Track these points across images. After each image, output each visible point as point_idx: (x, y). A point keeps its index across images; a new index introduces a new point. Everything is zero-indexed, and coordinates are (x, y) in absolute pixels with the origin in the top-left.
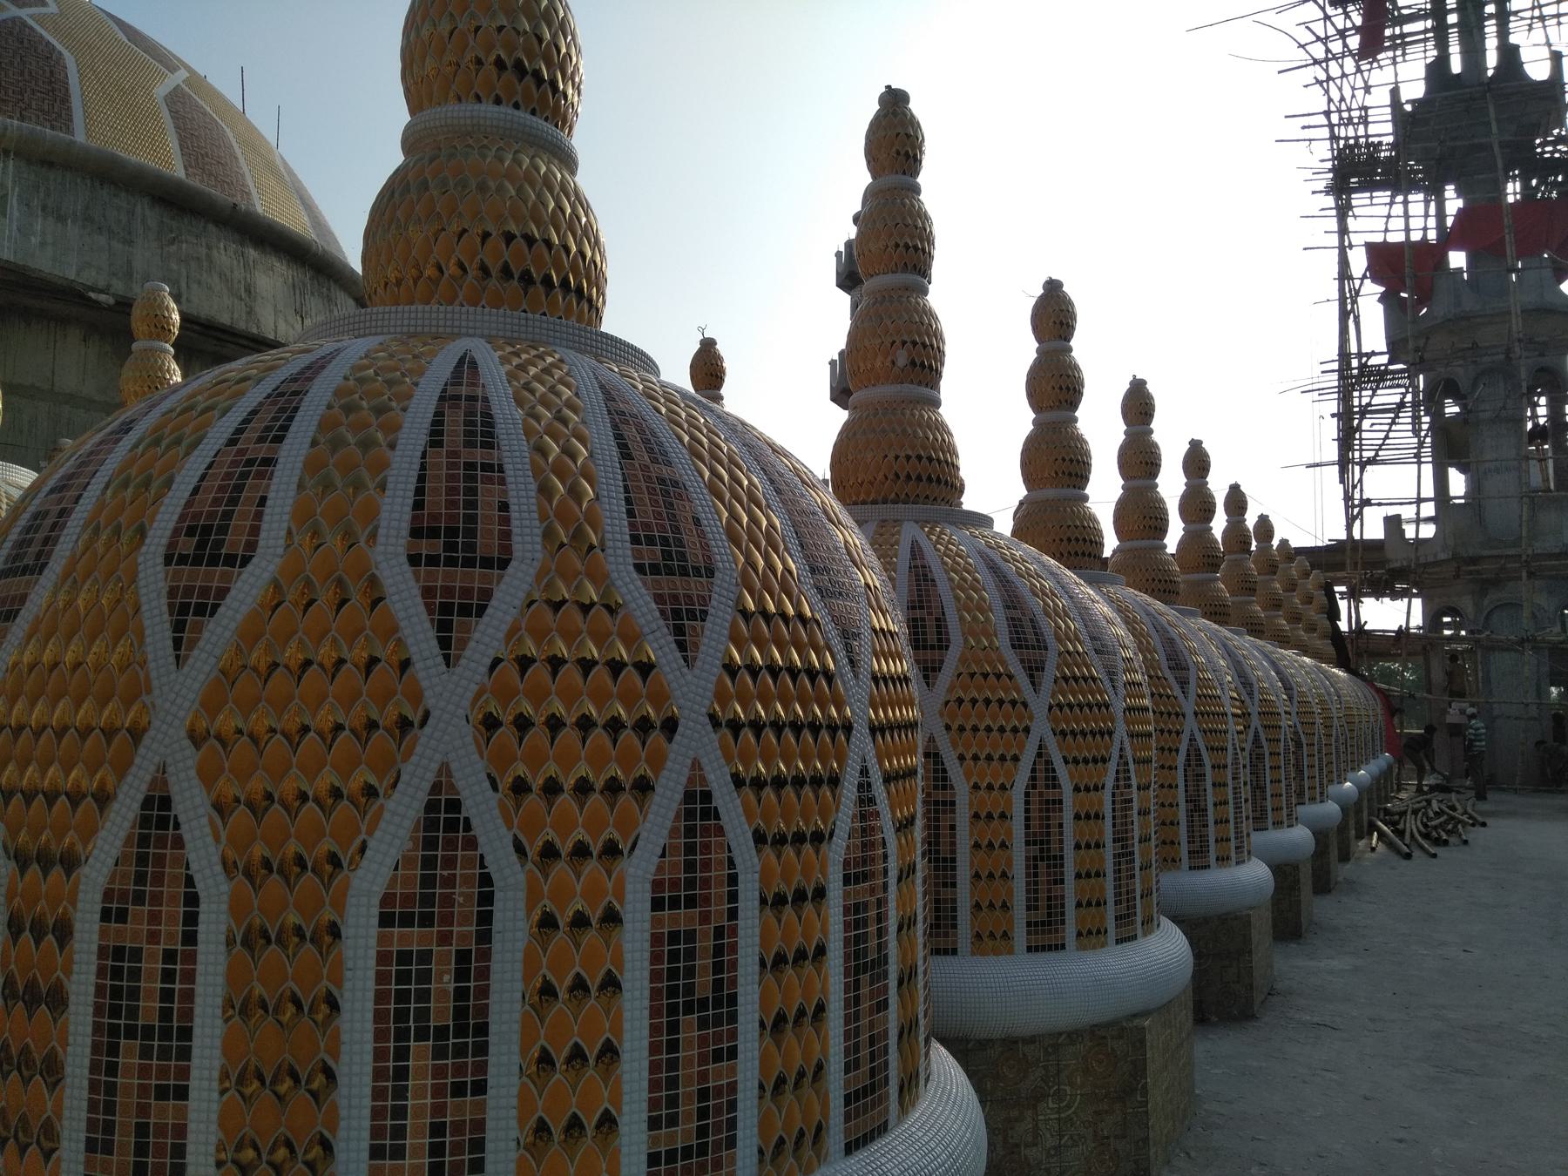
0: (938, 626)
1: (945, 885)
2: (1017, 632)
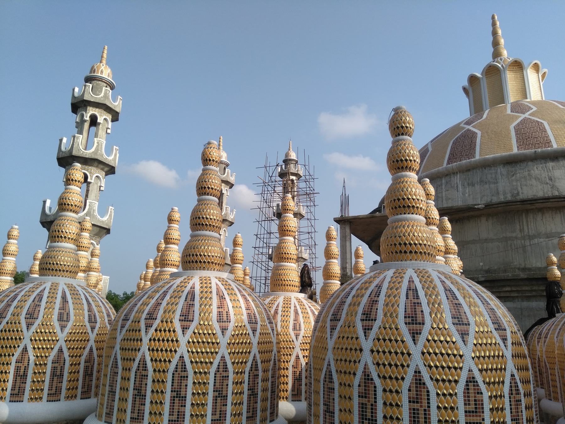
1: (224, 405)
2: (250, 318)
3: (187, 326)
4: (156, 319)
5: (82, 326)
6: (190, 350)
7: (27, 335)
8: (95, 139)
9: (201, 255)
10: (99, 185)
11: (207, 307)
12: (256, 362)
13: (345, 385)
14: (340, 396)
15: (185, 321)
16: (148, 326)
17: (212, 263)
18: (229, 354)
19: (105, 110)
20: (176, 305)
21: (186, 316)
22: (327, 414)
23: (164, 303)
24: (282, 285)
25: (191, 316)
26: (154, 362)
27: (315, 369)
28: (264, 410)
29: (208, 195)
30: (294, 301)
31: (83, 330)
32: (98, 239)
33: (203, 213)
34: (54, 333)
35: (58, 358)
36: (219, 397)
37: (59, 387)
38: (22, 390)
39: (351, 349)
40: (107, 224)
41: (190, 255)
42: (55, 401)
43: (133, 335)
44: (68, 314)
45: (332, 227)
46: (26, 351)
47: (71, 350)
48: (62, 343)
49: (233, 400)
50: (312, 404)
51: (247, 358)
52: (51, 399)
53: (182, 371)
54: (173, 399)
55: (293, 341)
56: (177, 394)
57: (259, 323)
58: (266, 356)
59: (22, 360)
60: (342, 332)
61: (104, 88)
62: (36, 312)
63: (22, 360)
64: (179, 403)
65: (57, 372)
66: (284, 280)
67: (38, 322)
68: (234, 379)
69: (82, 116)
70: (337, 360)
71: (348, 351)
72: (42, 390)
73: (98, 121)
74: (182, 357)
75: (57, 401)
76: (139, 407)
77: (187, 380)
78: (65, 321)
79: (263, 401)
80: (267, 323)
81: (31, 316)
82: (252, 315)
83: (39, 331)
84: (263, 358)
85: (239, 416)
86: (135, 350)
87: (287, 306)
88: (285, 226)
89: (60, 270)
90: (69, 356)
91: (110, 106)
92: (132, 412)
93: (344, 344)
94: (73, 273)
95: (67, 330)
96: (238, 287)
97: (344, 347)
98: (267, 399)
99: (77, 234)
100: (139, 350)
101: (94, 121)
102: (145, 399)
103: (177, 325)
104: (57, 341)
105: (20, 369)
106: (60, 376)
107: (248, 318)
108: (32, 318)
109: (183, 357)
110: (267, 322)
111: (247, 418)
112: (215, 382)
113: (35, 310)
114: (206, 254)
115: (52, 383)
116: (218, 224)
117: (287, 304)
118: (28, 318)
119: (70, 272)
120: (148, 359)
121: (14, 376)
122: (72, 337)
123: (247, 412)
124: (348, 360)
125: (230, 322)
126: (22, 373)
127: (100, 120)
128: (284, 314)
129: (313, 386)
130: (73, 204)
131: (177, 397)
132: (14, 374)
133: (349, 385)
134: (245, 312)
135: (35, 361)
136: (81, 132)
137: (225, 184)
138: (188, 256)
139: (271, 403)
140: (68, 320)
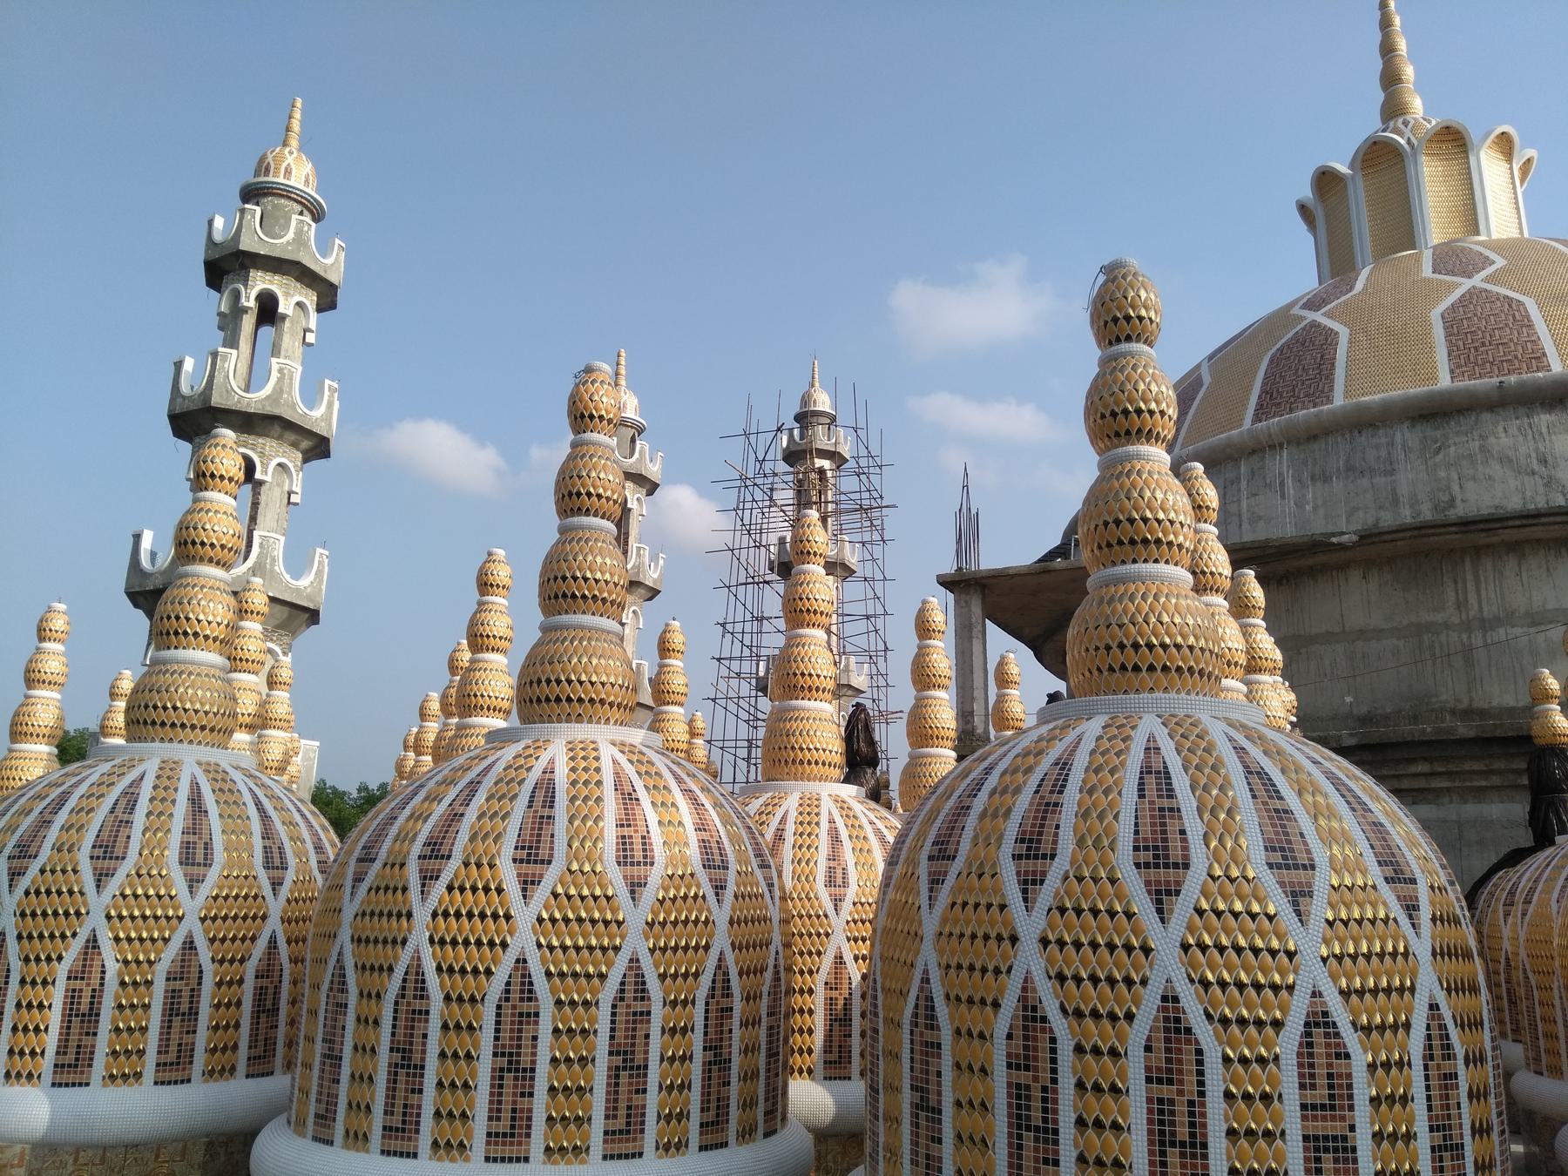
0: (644, 844)
1: (637, 1092)
3: (534, 875)
4: (449, 857)
5: (246, 877)
6: (542, 941)
7: (98, 903)
8: (274, 360)
9: (569, 682)
10: (286, 488)
11: (590, 823)
12: (726, 974)
13: (970, 1034)
14: (958, 1066)
15: (528, 862)
16: (428, 878)
17: (602, 702)
18: (652, 951)
19: (298, 279)
20: (503, 819)
21: (530, 848)
22: (923, 1114)
23: (471, 814)
24: (794, 761)
25: (545, 848)
26: (446, 976)
27: (886, 991)
28: (748, 1104)
29: (587, 513)
30: (827, 805)
31: (250, 888)
32: (286, 639)
33: (575, 565)
34: (171, 898)
35: (182, 967)
36: (625, 1069)
37: (187, 1044)
38: (85, 1053)
39: (986, 937)
40: (309, 598)
41: (539, 682)
42: (176, 1082)
43: (386, 902)
44: (208, 846)
45: (931, 599)
46: (94, 947)
47: (217, 943)
48: (192, 925)
49: (663, 1076)
50: (881, 1086)
51: (701, 962)
52: (167, 1076)
53: (522, 1000)
54: (498, 1075)
55: (826, 916)
56: (510, 1062)
57: (733, 866)
58: (752, 958)
59: (83, 972)
60: (960, 889)
61: (295, 217)
62: (121, 839)
63: (83, 972)
64: (515, 1086)
65: (179, 1003)
66: (801, 749)
67: (126, 867)
68: (666, 1019)
69: (236, 296)
70: (948, 967)
71: (979, 942)
72: (141, 1053)
73: (281, 309)
74: (521, 961)
75: (182, 1082)
76: (406, 1098)
77: (536, 1023)
78: (199, 864)
79: (745, 1079)
80: (755, 866)
81: (107, 852)
82: (714, 845)
83: (128, 892)
84: (744, 962)
85: (679, 1122)
86: (394, 942)
87: (808, 819)
88: (801, 599)
89: (183, 726)
90: (213, 960)
91: (313, 267)
92: (386, 1113)
93: (968, 922)
94: (219, 731)
95: (205, 890)
96: (675, 767)
97: (968, 933)
98: (755, 1075)
99: (227, 626)
100: (404, 942)
101: (268, 311)
102: (422, 1076)
103: (508, 875)
104: (180, 919)
105: (80, 997)
106: (190, 1014)
107: (701, 853)
108: (111, 858)
109: (525, 961)
110: (754, 862)
111: (702, 1125)
112: (613, 1030)
113: (116, 836)
114: (584, 678)
115: (169, 1033)
116: (618, 596)
117: (809, 814)
118: (98, 858)
119: (212, 730)
120: (429, 966)
121: (63, 1015)
122: (220, 909)
123: (702, 1110)
124: (978, 966)
125: (652, 864)
126: (84, 1008)
127: (286, 306)
128: (800, 841)
129: (881, 1039)
130: (215, 541)
131: (509, 1071)
132: (64, 1009)
133: (982, 1036)
134: (692, 837)
135: (120, 974)
136: (232, 342)
137: (635, 483)
138: (535, 685)
139: (767, 1085)
140: (207, 864)
